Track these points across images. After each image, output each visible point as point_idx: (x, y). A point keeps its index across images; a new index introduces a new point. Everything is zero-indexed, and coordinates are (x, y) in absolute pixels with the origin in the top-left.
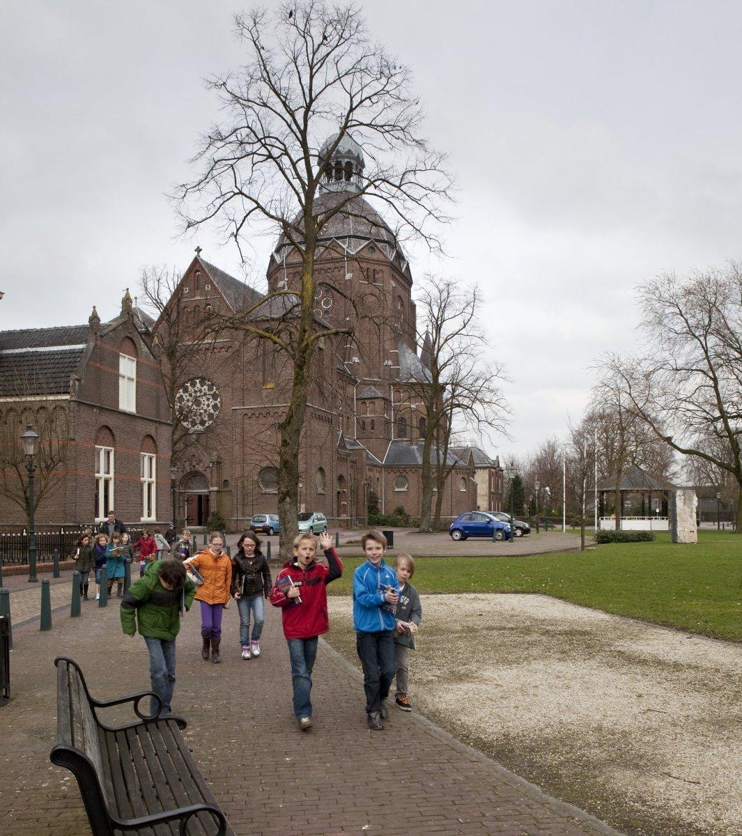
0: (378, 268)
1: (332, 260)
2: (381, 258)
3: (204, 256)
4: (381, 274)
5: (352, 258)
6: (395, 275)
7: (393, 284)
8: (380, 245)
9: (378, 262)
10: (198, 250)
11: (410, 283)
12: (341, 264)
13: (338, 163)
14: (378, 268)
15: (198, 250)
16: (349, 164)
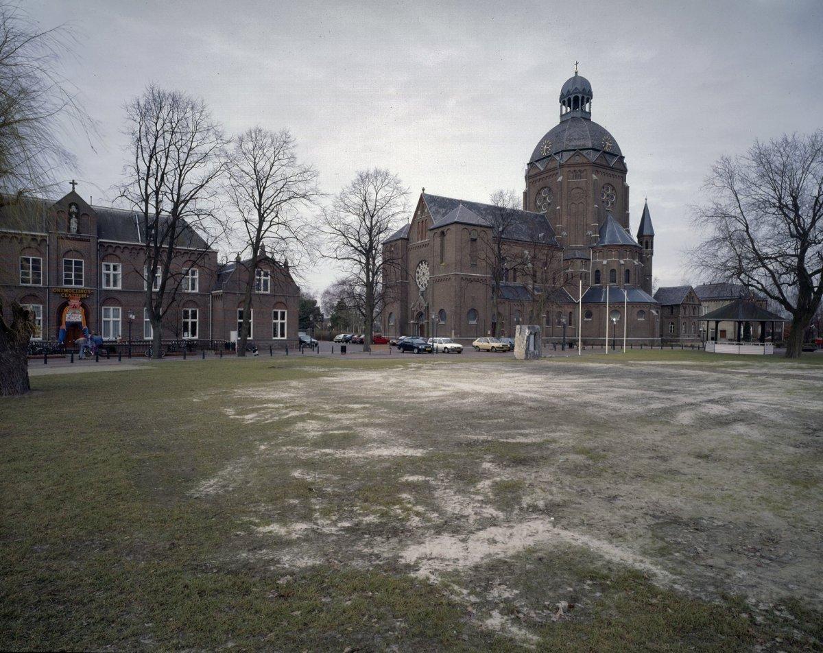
0: (582, 169)
1: (550, 170)
2: (585, 161)
3: (425, 192)
4: (585, 173)
5: (562, 166)
6: (599, 169)
7: (594, 177)
8: (584, 153)
9: (583, 164)
10: (423, 190)
11: (624, 171)
12: (555, 172)
13: (570, 99)
14: (582, 169)
15: (423, 190)
16: (576, 99)
